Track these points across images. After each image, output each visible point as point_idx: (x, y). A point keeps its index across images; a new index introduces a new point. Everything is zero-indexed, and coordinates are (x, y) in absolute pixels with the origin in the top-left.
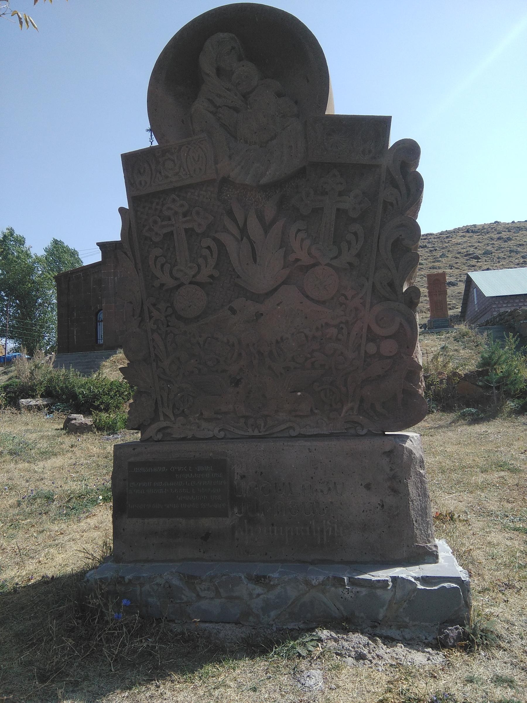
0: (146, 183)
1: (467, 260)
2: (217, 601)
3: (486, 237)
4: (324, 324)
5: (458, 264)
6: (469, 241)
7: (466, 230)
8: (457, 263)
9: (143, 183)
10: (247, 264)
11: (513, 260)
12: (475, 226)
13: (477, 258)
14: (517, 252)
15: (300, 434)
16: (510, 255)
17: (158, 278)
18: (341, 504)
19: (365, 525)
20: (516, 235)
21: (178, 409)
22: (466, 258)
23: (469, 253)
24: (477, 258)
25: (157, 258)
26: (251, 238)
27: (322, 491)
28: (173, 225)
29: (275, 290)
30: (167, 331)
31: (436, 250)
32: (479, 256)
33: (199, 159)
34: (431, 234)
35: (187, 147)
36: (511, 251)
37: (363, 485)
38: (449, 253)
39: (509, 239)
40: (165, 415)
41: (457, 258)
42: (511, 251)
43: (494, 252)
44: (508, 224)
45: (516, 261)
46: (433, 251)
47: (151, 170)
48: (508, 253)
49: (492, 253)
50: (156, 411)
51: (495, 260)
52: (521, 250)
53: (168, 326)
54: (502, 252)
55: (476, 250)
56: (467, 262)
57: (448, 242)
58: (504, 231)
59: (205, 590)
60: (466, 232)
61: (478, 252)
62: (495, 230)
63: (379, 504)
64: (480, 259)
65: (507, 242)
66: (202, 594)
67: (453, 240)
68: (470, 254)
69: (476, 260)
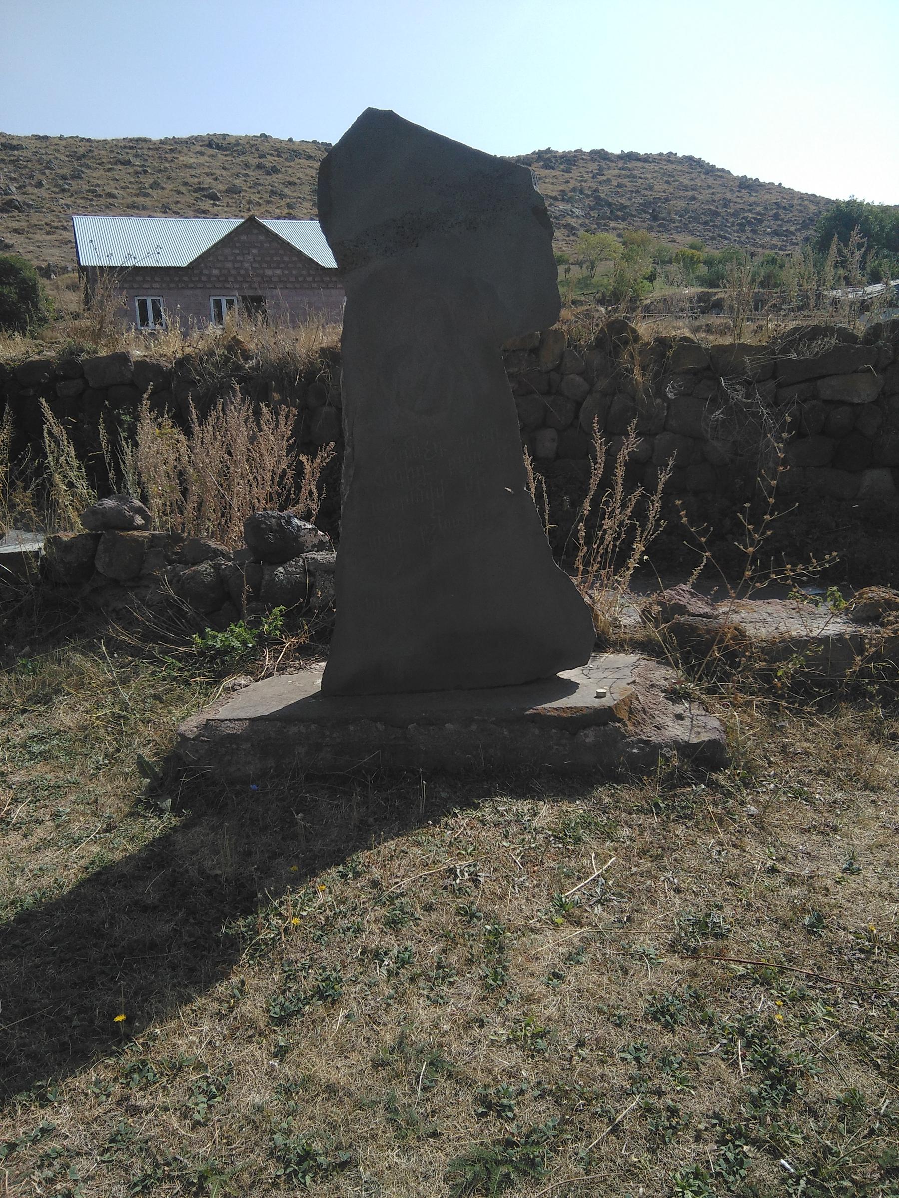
1: (197, 199)
3: (238, 160)
5: (179, 205)
6: (208, 164)
7: (207, 142)
8: (177, 202)
11: (271, 208)
12: (224, 136)
13: (214, 197)
14: (282, 196)
16: (269, 199)
20: (288, 164)
22: (196, 194)
23: (202, 186)
24: (214, 197)
31: (146, 172)
32: (218, 194)
34: (145, 140)
36: (273, 193)
38: (170, 182)
39: (275, 170)
41: (179, 192)
42: (273, 193)
43: (246, 191)
44: (281, 142)
45: (277, 210)
46: (141, 173)
48: (266, 196)
49: (240, 192)
51: (242, 205)
52: (289, 193)
54: (259, 192)
55: (214, 183)
56: (195, 202)
57: (172, 160)
58: (272, 155)
60: (207, 146)
61: (219, 187)
62: (257, 150)
64: (219, 199)
65: (271, 174)
67: (181, 158)
68: (203, 189)
69: (212, 202)
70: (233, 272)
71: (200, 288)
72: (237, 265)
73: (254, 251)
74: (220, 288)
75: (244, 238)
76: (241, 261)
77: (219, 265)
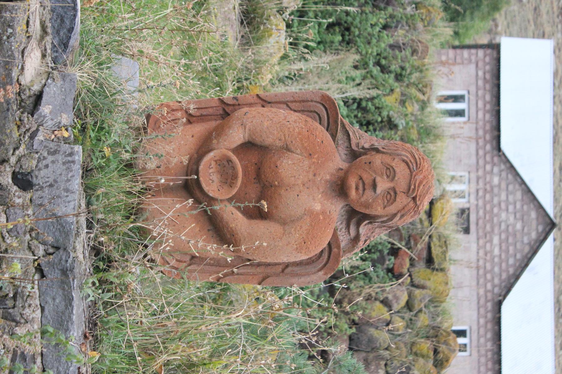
70: (496, 200)
71: (478, 162)
72: (503, 206)
73: (519, 226)
75: (533, 215)
76: (507, 210)
77: (503, 185)
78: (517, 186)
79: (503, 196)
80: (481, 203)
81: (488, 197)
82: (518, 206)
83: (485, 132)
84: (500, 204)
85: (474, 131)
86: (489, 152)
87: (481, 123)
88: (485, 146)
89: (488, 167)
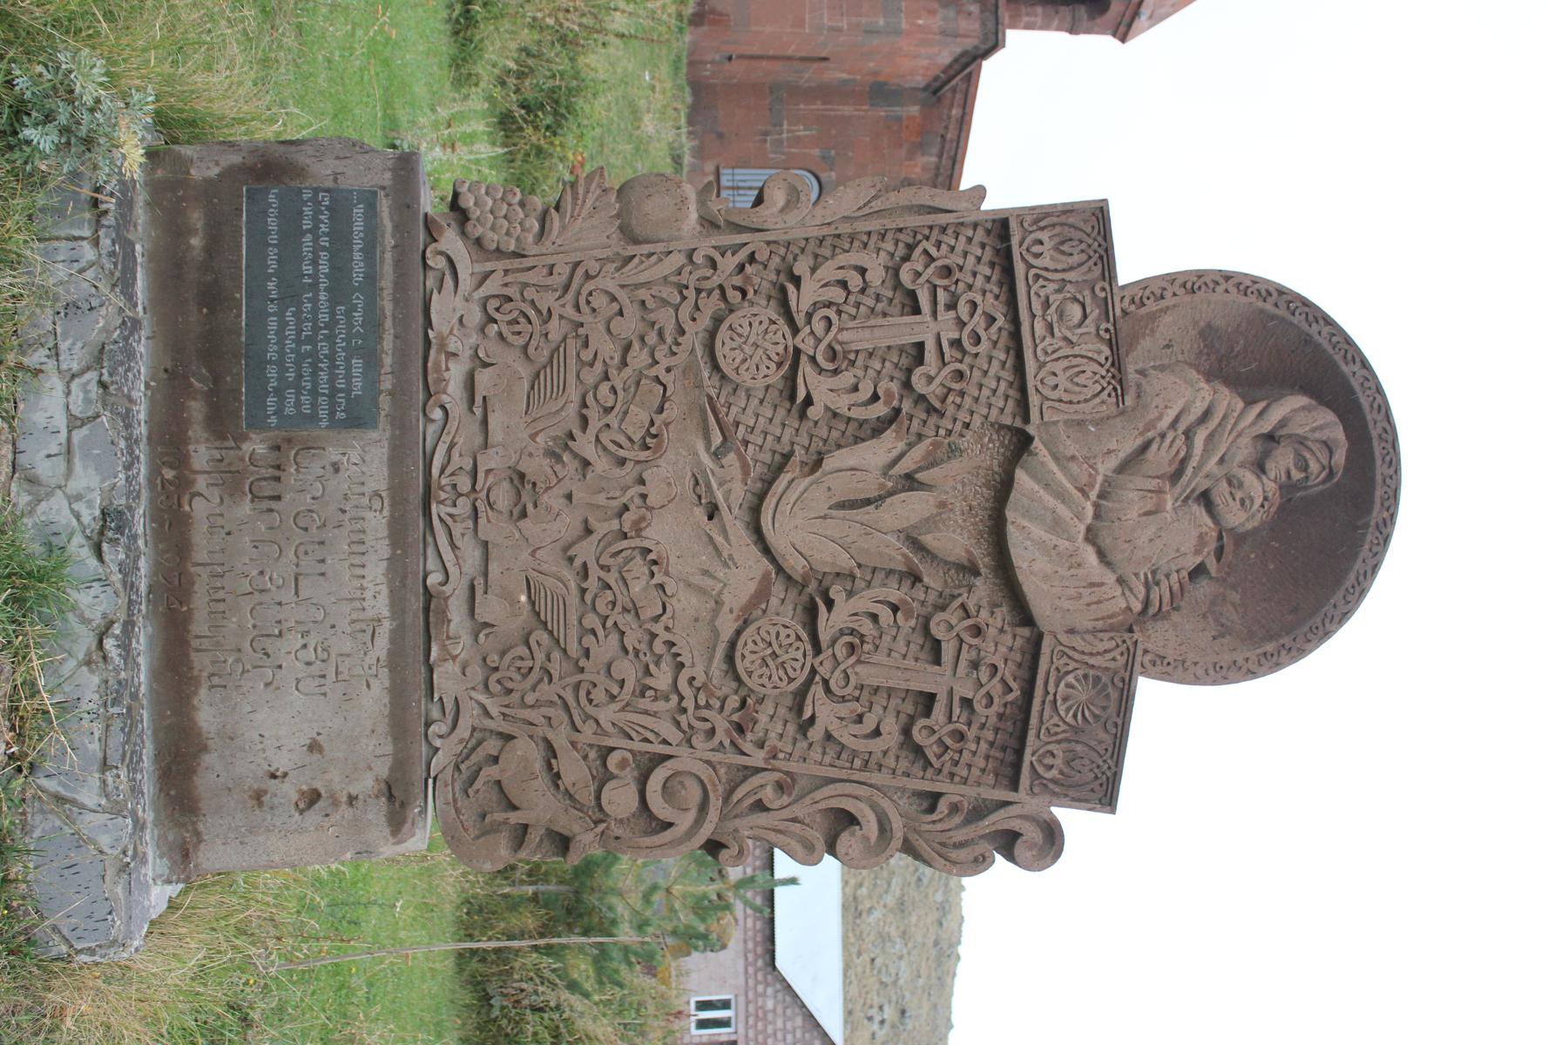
0: (1037, 256)
2: (61, 422)
4: (679, 659)
9: (1036, 249)
10: (829, 489)
15: (431, 596)
17: (813, 270)
18: (277, 688)
19: (232, 739)
21: (497, 310)
25: (862, 271)
26: (888, 500)
27: (305, 646)
28: (934, 314)
29: (767, 551)
30: (687, 288)
33: (1077, 384)
35: (1107, 359)
37: (318, 738)
40: (486, 276)
47: (1064, 270)
50: (499, 253)
53: (699, 291)
59: (86, 392)
63: (277, 770)
66: (74, 386)
70: (770, 1029)
71: (747, 983)
72: (780, 1035)
74: (747, 1011)
77: (780, 1010)
78: (797, 1010)
79: (780, 1024)
80: (751, 1033)
81: (760, 1025)
82: (799, 1034)
83: (756, 943)
84: (775, 1034)
85: (742, 943)
86: (760, 969)
87: (750, 933)
88: (756, 961)
89: (760, 988)
